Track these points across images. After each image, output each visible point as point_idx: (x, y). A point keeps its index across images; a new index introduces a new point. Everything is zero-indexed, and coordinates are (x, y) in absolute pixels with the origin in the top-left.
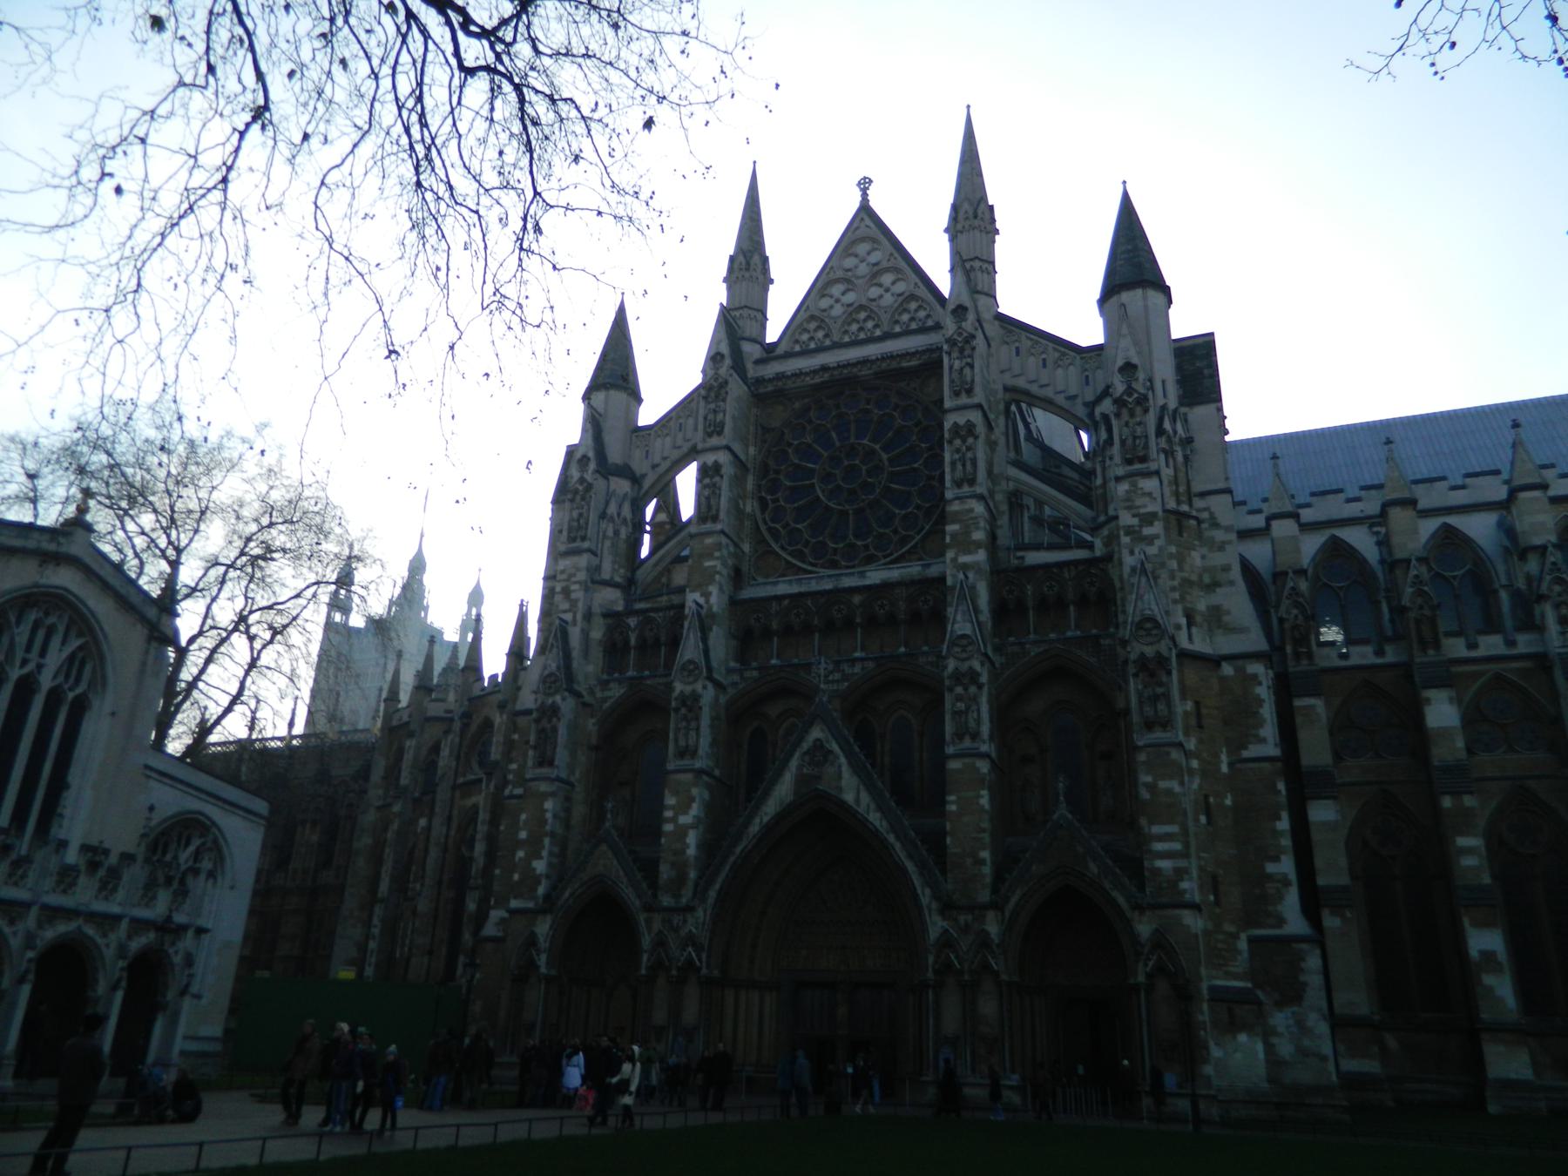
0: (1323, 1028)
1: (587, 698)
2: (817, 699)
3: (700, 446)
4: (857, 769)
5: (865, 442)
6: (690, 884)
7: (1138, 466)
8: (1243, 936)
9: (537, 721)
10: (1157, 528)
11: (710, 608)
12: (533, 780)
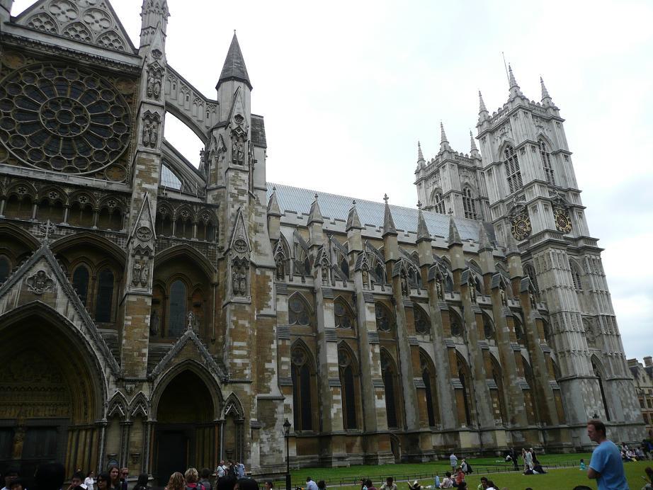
0: (282, 440)
2: (42, 246)
7: (238, 166)
8: (256, 397)
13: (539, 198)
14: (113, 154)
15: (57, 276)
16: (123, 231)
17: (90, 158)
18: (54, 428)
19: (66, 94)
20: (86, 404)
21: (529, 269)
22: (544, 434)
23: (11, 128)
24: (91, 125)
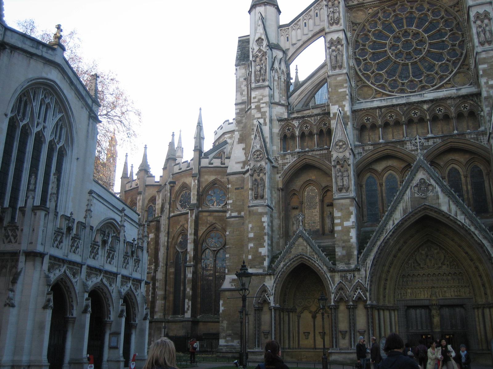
1: (275, 164)
2: (418, 158)
3: (327, 30)
5: (413, 28)
6: (356, 257)
9: (252, 175)
11: (345, 113)
12: (252, 206)
14: (455, 64)
15: (435, 181)
16: (482, 128)
17: (436, 73)
18: (461, 306)
19: (403, 27)
20: (484, 285)
23: (371, 70)
24: (430, 43)
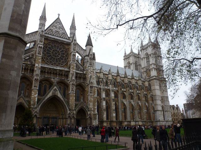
4: (60, 93)
7: (91, 66)
10: (92, 73)
13: (153, 68)
21: (150, 85)
22: (150, 122)
